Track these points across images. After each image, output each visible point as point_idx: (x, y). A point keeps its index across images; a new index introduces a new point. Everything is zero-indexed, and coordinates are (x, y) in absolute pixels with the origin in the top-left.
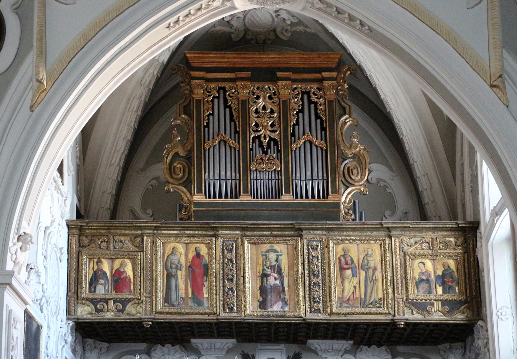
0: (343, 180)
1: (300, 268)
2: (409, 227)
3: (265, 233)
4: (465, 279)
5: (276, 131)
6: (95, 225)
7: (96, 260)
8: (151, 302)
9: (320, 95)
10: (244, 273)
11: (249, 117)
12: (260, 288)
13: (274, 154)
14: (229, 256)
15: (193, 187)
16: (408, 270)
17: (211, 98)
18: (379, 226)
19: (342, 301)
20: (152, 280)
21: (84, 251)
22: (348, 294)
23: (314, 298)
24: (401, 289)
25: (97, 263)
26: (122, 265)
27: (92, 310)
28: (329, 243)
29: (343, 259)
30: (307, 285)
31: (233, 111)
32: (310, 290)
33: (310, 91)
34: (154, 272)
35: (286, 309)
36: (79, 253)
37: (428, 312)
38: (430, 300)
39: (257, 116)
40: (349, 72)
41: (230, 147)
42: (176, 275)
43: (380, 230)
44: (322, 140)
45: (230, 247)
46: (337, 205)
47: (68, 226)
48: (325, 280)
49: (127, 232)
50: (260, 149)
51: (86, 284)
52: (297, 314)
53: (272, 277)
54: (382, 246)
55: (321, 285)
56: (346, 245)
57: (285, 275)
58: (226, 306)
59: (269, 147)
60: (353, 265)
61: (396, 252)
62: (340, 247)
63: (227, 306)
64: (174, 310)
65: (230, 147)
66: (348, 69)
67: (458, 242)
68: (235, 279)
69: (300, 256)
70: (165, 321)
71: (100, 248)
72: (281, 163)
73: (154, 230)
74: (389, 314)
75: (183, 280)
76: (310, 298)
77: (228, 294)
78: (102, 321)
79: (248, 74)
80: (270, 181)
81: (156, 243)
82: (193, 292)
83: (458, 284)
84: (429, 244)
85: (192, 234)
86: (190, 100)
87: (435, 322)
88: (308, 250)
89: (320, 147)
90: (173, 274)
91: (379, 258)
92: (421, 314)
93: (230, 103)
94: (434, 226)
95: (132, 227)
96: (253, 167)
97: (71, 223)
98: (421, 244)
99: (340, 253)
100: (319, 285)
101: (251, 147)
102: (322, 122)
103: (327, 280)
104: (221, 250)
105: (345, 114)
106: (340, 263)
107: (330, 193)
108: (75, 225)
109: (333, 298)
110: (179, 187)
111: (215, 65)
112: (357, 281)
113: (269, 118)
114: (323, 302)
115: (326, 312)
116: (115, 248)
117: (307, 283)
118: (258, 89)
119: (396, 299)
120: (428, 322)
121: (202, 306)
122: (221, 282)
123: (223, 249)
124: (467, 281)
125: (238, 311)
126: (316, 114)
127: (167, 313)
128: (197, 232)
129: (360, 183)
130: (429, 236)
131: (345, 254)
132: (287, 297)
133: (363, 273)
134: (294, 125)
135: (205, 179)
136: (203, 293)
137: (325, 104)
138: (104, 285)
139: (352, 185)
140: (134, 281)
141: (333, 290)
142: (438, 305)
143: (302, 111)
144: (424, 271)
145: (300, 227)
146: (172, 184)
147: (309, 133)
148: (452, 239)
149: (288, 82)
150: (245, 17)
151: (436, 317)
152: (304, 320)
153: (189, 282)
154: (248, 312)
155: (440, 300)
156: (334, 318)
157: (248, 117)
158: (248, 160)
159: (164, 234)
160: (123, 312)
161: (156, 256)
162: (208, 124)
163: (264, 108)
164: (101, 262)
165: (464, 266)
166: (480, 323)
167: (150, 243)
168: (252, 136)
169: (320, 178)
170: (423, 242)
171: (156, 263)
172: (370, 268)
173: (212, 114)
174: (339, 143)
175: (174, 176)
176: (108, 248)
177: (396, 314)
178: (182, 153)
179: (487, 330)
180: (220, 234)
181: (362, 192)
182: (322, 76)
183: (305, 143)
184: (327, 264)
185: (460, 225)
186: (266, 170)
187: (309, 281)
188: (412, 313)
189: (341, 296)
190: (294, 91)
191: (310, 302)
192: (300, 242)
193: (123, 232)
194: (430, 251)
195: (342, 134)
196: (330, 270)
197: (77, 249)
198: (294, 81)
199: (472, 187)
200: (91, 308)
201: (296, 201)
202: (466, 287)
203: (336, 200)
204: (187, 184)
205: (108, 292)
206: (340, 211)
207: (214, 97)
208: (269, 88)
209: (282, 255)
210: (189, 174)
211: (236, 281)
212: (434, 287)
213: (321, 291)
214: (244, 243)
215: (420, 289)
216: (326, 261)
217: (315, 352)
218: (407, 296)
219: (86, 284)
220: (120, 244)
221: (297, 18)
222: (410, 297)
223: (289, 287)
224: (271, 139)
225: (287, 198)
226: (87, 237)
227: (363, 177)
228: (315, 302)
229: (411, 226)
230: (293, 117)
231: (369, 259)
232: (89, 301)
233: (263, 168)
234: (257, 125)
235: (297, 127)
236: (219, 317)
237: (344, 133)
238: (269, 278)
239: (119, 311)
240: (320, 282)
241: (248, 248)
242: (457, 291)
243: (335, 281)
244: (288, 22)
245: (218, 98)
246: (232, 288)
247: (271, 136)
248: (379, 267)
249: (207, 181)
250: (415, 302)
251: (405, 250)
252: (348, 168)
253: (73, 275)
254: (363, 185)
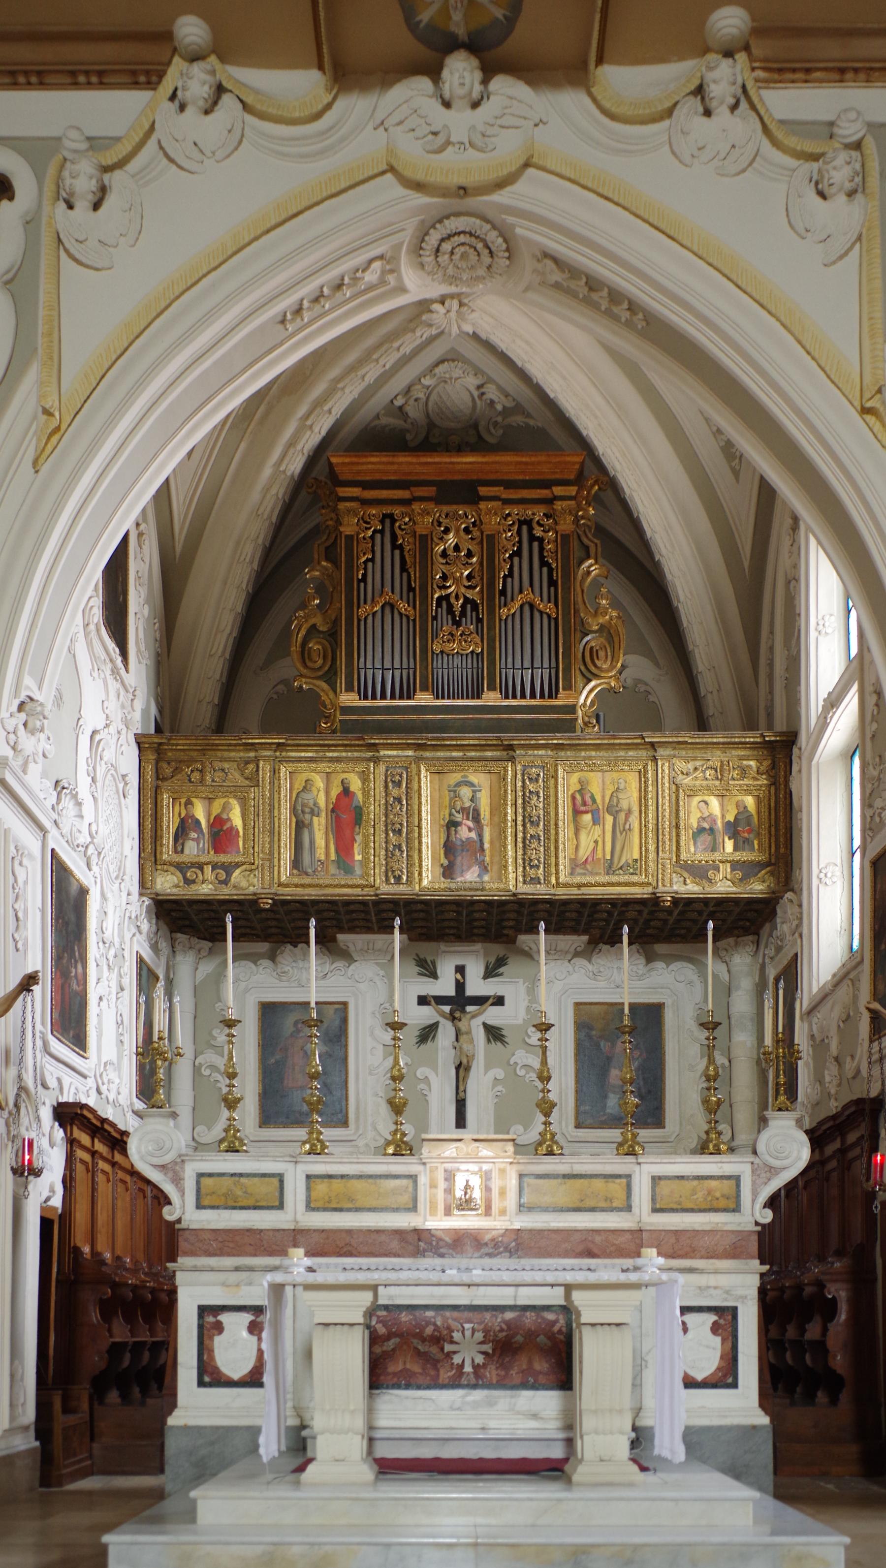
0: (583, 668)
1: (509, 811)
2: (686, 743)
3: (454, 754)
4: (770, 827)
5: (475, 587)
6: (181, 742)
7: (183, 801)
8: (271, 868)
9: (548, 525)
10: (420, 820)
11: (432, 564)
12: (445, 845)
13: (472, 624)
14: (395, 792)
15: (339, 681)
16: (682, 814)
17: (370, 533)
18: (639, 741)
19: (575, 865)
20: (273, 832)
22: (584, 853)
23: (531, 860)
24: (668, 845)
25: (186, 805)
26: (226, 807)
27: (180, 881)
28: (556, 771)
29: (578, 797)
30: (519, 840)
31: (406, 553)
32: (524, 847)
33: (531, 520)
34: (276, 819)
35: (486, 878)
36: (157, 790)
37: (710, 880)
38: (713, 861)
39: (444, 561)
40: (596, 487)
41: (401, 614)
42: (311, 823)
43: (640, 749)
44: (549, 602)
45: (397, 778)
46: (572, 709)
47: (139, 744)
48: (549, 831)
49: (233, 754)
50: (449, 617)
51: (168, 839)
52: (502, 886)
53: (464, 826)
54: (642, 774)
55: (542, 838)
56: (585, 774)
57: (486, 823)
58: (390, 874)
59: (463, 613)
60: (595, 807)
61: (663, 784)
62: (575, 778)
64: (307, 880)
65: (401, 614)
66: (596, 482)
67: (762, 768)
68: (405, 830)
69: (509, 792)
70: (294, 897)
71: (190, 780)
72: (482, 641)
73: (275, 751)
74: (649, 884)
75: (322, 832)
76: (524, 860)
77: (393, 855)
78: (195, 897)
79: (431, 491)
80: (464, 671)
81: (279, 773)
82: (337, 852)
83: (758, 835)
84: (716, 771)
85: (336, 757)
86: (336, 537)
87: (720, 896)
88: (523, 782)
89: (547, 614)
90: (306, 822)
91: (635, 795)
92: (697, 884)
93: (400, 542)
94: (725, 740)
95: (240, 745)
96: (437, 648)
97: (143, 740)
98: (704, 772)
99: (575, 786)
100: (539, 840)
101: (434, 614)
102: (550, 571)
103: (553, 832)
104: (383, 783)
105: (588, 557)
106: (574, 804)
107: (561, 690)
108: (150, 744)
109: (561, 861)
110: (315, 681)
111: (377, 477)
112: (600, 832)
113: (464, 565)
114: (544, 867)
115: (549, 882)
116: (213, 781)
117: (520, 835)
118: (447, 516)
119: (660, 861)
120: (709, 896)
121: (352, 874)
122: (383, 836)
123: (386, 782)
124: (773, 829)
125: (409, 882)
126: (542, 557)
127: (296, 886)
128: (344, 754)
129: (610, 674)
130: (716, 757)
131: (582, 789)
132: (487, 859)
133: (609, 819)
134: (505, 577)
135: (358, 668)
136: (354, 854)
137: (556, 541)
138: (197, 840)
139: (597, 677)
140: (244, 834)
141: (561, 847)
143: (518, 553)
144: (707, 814)
145: (511, 743)
146: (305, 677)
147: (530, 589)
148: (752, 763)
149: (497, 504)
150: (428, 398)
151: (722, 889)
152: (514, 895)
153: (331, 836)
154: (425, 883)
155: (730, 862)
156: (560, 891)
157: (429, 562)
158: (430, 635)
159: (292, 757)
160: (227, 885)
161: (279, 794)
162: (365, 575)
163: (457, 548)
164: (192, 803)
165: (770, 805)
166: (789, 895)
167: (270, 771)
168: (436, 596)
169: (546, 665)
170: (707, 768)
171: (279, 804)
172: (621, 810)
173: (372, 560)
174: (577, 606)
175: (309, 664)
176: (202, 781)
177: (660, 884)
179: (800, 906)
180: (382, 757)
181: (611, 688)
182: (553, 493)
183: (522, 606)
184: (552, 805)
185: (767, 739)
186: (457, 652)
187: (524, 833)
188: (685, 884)
189: (573, 857)
190: (505, 519)
191: (524, 868)
192: (510, 769)
193: (226, 754)
194: (717, 783)
195: (583, 591)
196: (557, 814)
197: (154, 784)
198: (507, 502)
199: (786, 679)
200: (176, 876)
201: (506, 703)
202: (770, 840)
203: (570, 702)
204: (330, 677)
205: (204, 853)
206: (576, 719)
207: (375, 532)
208: (465, 514)
209: (480, 791)
210: (334, 659)
211: (407, 834)
212: (721, 841)
213: (542, 849)
214: (420, 771)
215: (699, 844)
216: (552, 799)
218: (678, 856)
219: (168, 839)
220: (221, 774)
221: (514, 400)
222: (682, 858)
223: (492, 843)
224: (466, 599)
225: (491, 698)
226: (169, 763)
227: (614, 663)
228: (531, 867)
229: (690, 741)
230: (503, 563)
231: (621, 796)
232: (175, 866)
233: (454, 649)
234: (444, 577)
235: (509, 580)
236: (378, 892)
237: (585, 591)
238: (459, 828)
239: (221, 882)
240: (541, 834)
242: (756, 847)
243: (565, 832)
244: (499, 407)
245: (382, 532)
246: (400, 845)
247: (468, 595)
248: (635, 809)
249: (362, 672)
250: (689, 865)
251: (678, 781)
252: (592, 648)
253: (148, 824)
254: (614, 676)
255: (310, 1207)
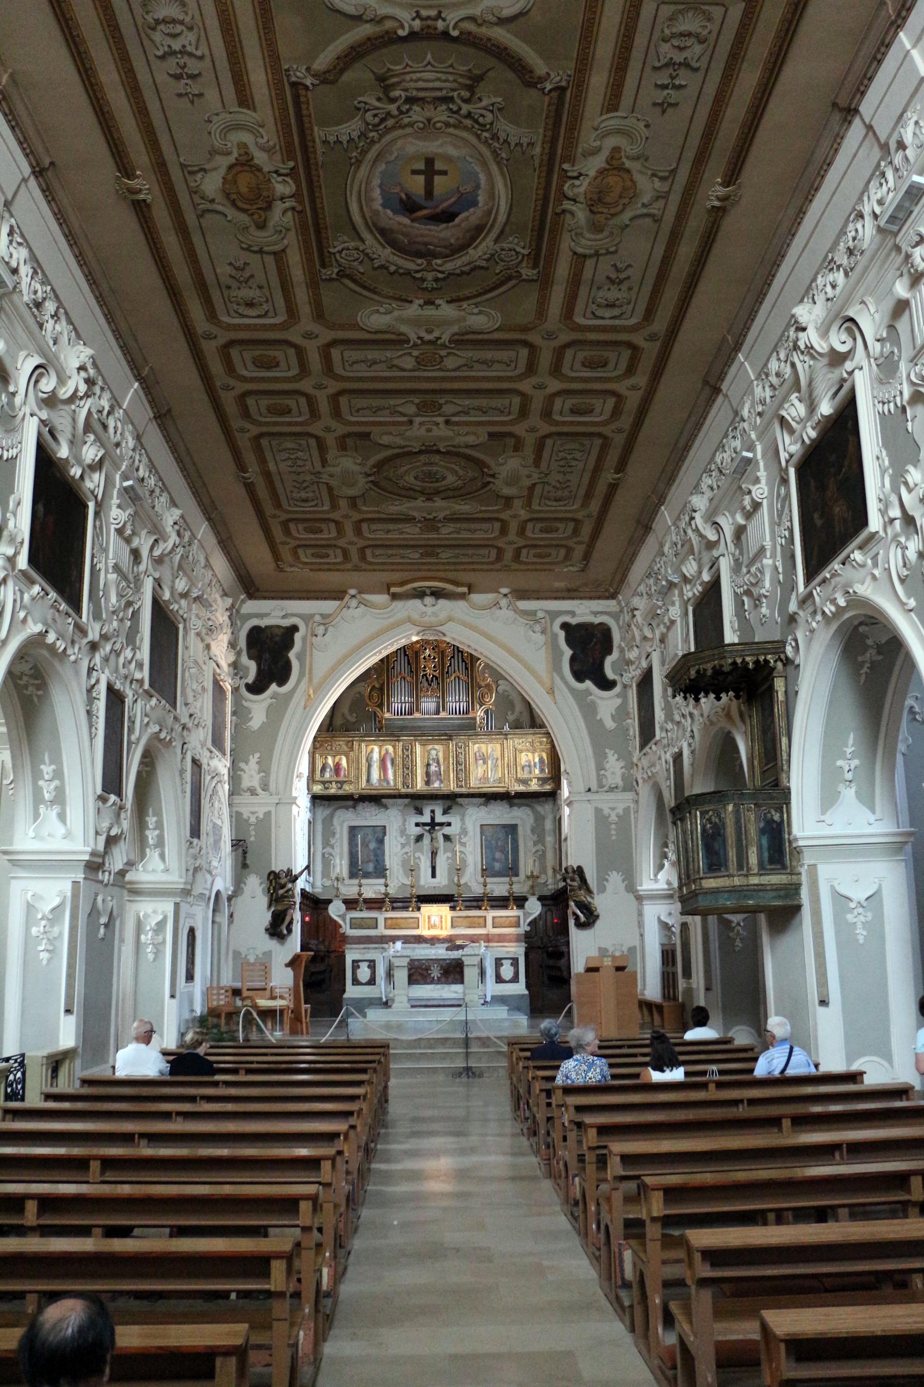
20: (358, 769)
21: (317, 751)
46: (475, 719)
51: (318, 772)
54: (502, 745)
63: (405, 784)
142: (535, 781)
178: (377, 686)
217: (461, 805)
219: (318, 772)
241: (418, 748)
255: (386, 928)
